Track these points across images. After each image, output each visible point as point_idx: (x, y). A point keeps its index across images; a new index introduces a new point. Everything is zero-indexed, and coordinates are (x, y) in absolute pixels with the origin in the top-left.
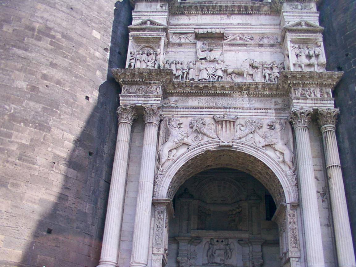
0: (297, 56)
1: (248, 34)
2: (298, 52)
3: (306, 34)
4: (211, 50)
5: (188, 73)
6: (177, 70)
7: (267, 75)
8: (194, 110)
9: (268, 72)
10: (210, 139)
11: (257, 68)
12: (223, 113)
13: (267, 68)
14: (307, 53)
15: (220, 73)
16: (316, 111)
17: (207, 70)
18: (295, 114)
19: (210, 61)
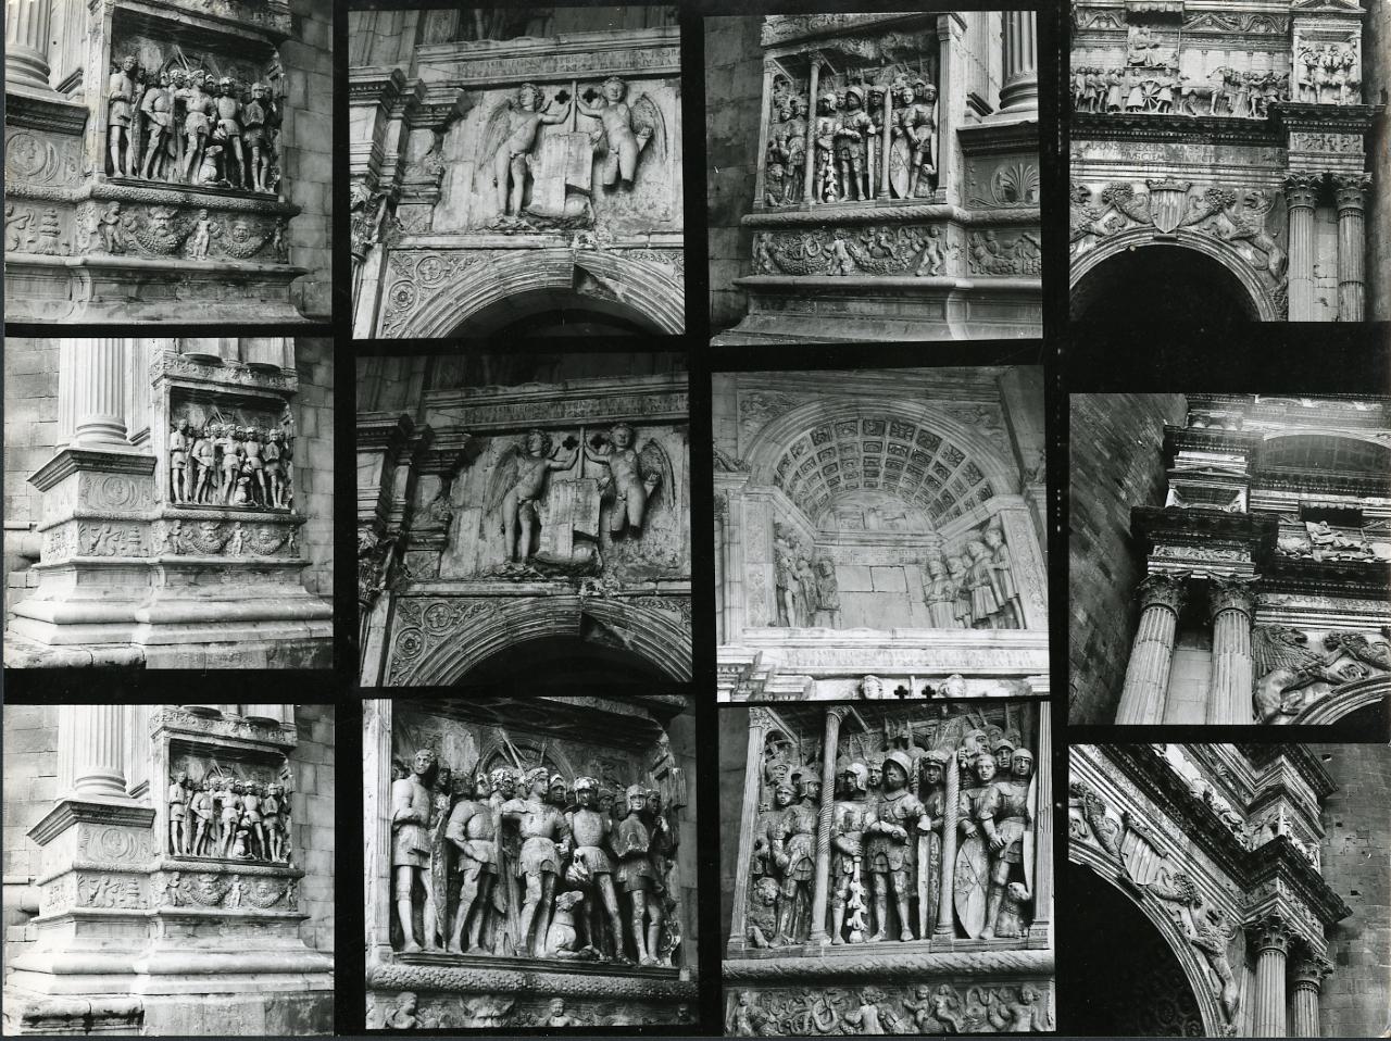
0: (1310, 68)
1: (1229, 13)
2: (1311, 62)
3: (1330, 22)
4: (1156, 46)
5: (1106, 94)
6: (1088, 86)
7: (1254, 101)
8: (1112, 167)
9: (1256, 94)
10: (1139, 225)
11: (1239, 85)
12: (1164, 175)
13: (1256, 86)
14: (1328, 63)
15: (1166, 95)
16: (1328, 177)
17: (1144, 89)
18: (1289, 183)
19: (1151, 69)
